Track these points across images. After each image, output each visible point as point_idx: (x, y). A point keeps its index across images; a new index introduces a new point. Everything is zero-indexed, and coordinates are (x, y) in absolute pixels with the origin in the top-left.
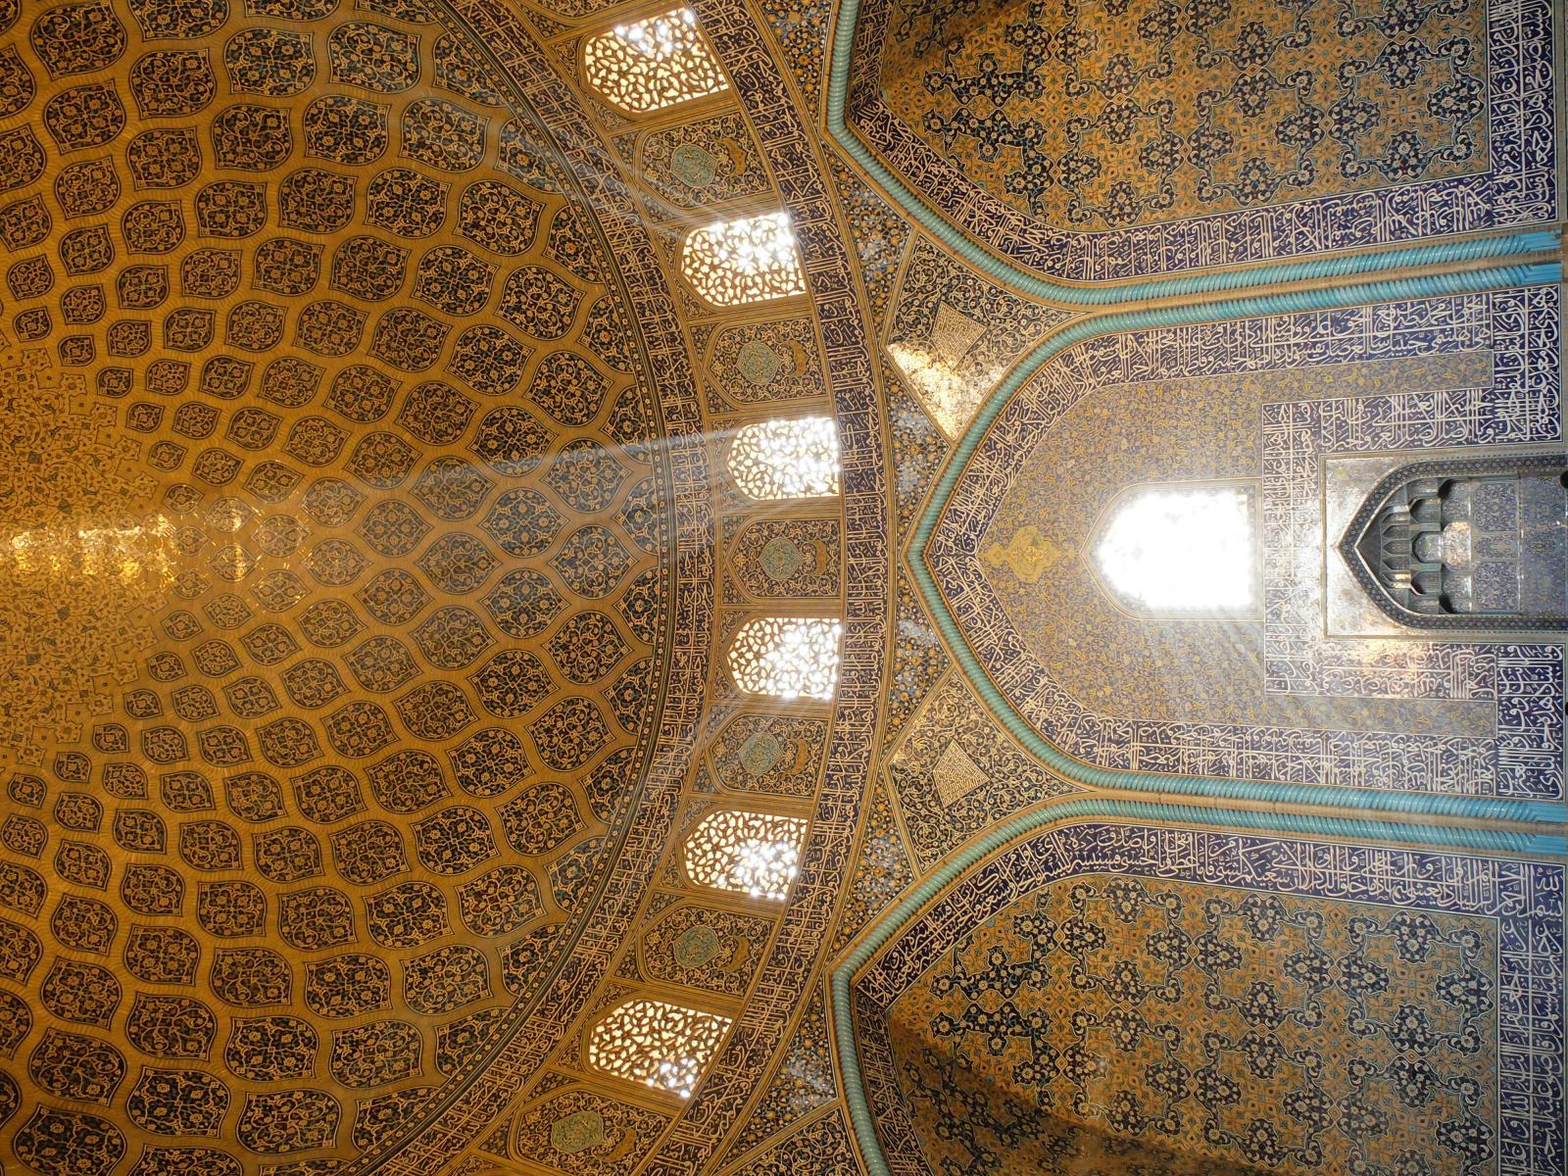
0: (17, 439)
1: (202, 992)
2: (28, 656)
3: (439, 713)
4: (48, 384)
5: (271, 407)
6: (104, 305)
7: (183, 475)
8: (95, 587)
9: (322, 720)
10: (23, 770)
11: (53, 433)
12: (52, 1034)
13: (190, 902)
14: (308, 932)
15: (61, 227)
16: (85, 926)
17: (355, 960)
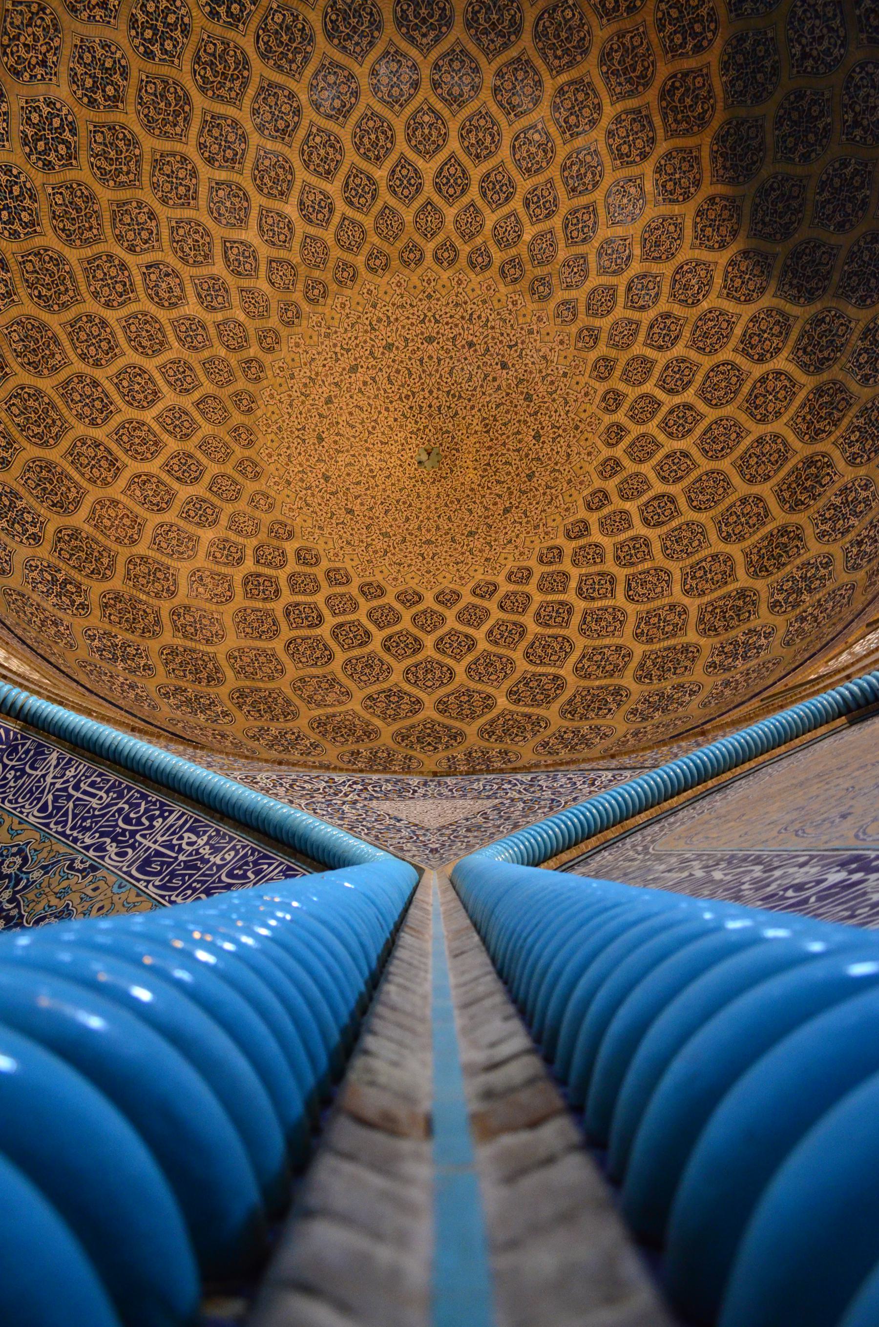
0: (404, 541)
1: (199, 100)
2: (332, 402)
3: (32, 345)
4: (410, 575)
5: (260, 605)
6: (416, 626)
7: (290, 547)
8: (308, 460)
9: (123, 354)
10: (320, 309)
11: (386, 552)
12: (297, 76)
13: (203, 192)
14: (121, 144)
15: (483, 645)
16: (273, 174)
17: (92, 102)
